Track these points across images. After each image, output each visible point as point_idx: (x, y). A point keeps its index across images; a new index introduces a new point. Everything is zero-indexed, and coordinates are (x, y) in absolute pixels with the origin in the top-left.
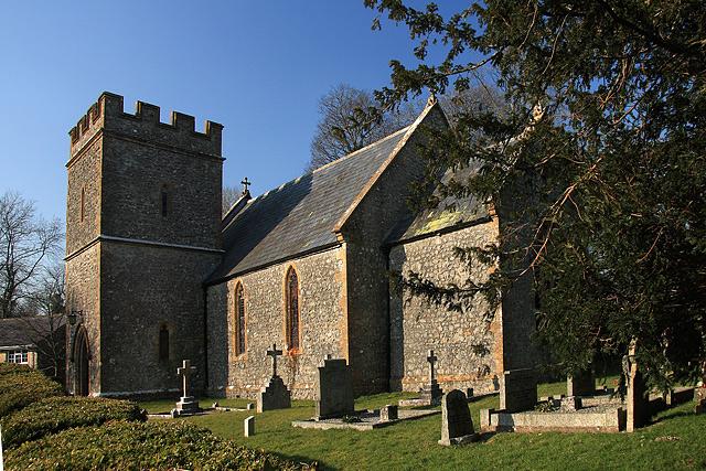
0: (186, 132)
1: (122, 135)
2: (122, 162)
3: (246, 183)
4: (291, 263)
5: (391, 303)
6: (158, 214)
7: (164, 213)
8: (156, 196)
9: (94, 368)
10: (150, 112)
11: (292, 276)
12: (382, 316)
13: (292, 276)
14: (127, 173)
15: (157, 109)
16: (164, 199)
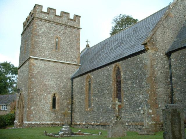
0: (66, 18)
1: (41, 19)
2: (41, 29)
3: (88, 42)
4: (117, 63)
5: (173, 81)
6: (54, 48)
7: (56, 48)
8: (53, 42)
9: (81, 93)
10: (53, 11)
11: (118, 71)
12: (168, 88)
13: (118, 71)
14: (42, 33)
15: (55, 10)
16: (57, 44)
